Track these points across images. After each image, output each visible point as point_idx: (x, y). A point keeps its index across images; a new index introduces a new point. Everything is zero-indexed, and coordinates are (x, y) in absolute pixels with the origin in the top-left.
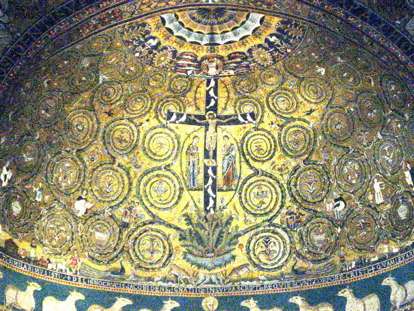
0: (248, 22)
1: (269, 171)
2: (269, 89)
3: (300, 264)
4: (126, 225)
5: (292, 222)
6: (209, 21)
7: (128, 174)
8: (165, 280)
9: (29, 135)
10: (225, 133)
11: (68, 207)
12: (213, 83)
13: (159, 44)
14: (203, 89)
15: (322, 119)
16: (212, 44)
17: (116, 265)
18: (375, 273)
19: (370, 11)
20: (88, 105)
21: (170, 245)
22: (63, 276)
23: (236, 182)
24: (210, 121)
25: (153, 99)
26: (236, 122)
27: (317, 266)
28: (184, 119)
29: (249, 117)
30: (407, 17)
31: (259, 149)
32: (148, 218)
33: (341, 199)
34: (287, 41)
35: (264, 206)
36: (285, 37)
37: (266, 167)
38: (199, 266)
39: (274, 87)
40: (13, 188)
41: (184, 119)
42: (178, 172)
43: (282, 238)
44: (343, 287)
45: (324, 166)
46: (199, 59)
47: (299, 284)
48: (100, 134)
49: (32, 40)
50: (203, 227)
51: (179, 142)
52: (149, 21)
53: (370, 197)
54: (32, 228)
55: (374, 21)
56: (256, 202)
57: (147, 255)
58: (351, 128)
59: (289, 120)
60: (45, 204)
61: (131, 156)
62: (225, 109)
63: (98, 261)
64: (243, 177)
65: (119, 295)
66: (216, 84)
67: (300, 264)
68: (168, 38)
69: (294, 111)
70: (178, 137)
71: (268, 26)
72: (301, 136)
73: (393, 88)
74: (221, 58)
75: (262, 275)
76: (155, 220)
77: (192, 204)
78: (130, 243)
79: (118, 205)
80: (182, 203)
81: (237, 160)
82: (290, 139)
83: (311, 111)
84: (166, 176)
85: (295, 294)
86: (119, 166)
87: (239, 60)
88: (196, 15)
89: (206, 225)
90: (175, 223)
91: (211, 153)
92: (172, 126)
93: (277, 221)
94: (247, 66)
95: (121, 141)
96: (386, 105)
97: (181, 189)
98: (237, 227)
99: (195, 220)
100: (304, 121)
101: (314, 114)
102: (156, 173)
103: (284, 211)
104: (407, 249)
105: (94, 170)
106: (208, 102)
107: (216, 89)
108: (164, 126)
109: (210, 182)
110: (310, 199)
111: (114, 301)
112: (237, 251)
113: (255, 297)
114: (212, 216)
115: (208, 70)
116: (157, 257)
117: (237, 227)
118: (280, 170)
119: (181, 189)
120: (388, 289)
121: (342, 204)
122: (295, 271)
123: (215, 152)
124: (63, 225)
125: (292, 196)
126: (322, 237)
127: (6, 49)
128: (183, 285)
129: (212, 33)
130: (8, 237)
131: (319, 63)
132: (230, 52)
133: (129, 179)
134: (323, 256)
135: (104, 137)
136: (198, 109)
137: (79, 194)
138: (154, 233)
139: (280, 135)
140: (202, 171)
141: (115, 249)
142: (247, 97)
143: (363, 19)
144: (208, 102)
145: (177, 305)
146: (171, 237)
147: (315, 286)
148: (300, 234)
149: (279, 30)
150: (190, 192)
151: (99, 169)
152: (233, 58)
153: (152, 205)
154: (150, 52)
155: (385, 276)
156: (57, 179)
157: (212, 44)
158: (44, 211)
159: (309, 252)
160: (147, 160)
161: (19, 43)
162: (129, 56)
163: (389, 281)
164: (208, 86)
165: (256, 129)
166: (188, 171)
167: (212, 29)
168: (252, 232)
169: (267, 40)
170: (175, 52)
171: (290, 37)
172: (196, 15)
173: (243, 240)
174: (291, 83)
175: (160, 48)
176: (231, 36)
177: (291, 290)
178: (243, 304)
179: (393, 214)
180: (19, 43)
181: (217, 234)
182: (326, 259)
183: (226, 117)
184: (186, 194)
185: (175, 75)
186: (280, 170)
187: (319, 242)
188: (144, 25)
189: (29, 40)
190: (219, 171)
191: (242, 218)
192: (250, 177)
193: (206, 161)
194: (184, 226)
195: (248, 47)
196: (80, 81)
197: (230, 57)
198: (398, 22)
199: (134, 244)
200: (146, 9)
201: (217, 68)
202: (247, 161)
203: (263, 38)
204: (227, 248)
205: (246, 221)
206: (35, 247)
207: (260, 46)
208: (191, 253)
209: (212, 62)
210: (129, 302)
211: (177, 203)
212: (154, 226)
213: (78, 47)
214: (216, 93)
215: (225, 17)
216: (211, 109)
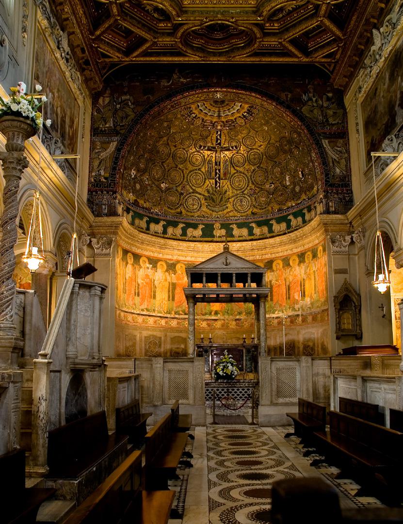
0: (235, 107)
1: (243, 171)
2: (243, 136)
3: (255, 210)
4: (182, 194)
5: (252, 193)
6: (218, 106)
7: (183, 172)
8: (198, 217)
9: (142, 156)
10: (224, 155)
11: (159, 187)
12: (219, 133)
13: (196, 116)
14: (215, 136)
15: (265, 149)
16: (219, 116)
17: (179, 210)
18: (285, 214)
19: (287, 103)
20: (166, 142)
21: (201, 202)
22: (157, 215)
23: (228, 176)
24: (218, 149)
25: (193, 140)
26: (228, 150)
27: (262, 211)
28: (206, 148)
29: (234, 148)
30: (302, 106)
31: (238, 162)
32: (191, 191)
33: (272, 183)
34: (251, 115)
35: (240, 186)
36: (250, 113)
37: (241, 169)
38: (213, 211)
39: (245, 135)
40: (136, 178)
41: (206, 148)
42: (204, 171)
43: (247, 199)
44: (271, 219)
45: (266, 169)
46: (213, 122)
47: (254, 218)
48: (171, 155)
49: (143, 116)
50: (214, 195)
51: (204, 158)
52: (192, 106)
53: (284, 183)
54: (144, 195)
55: (288, 107)
56: (237, 184)
57: (191, 206)
58: (278, 153)
59: (251, 149)
60: (149, 185)
61: (184, 164)
62: (224, 144)
63: (171, 209)
64: (232, 174)
65: (180, 222)
66: (221, 134)
67: (255, 210)
68: (200, 113)
69: (254, 145)
70: (204, 156)
71: (243, 108)
72: (257, 156)
73: (295, 136)
74: (223, 122)
75: (239, 215)
76: (194, 192)
77: (210, 185)
78: (184, 201)
79: (179, 185)
80: (206, 185)
81: (229, 166)
82: (252, 157)
83: (261, 146)
84: (200, 173)
85: (252, 222)
86: (179, 168)
87: (230, 123)
88: (212, 103)
89: (216, 194)
90: (203, 193)
91: (218, 164)
92: (201, 151)
93: (245, 192)
94: (234, 126)
95: (180, 158)
96: (292, 144)
97: (205, 179)
99: (211, 191)
100: (258, 150)
101: (262, 147)
102: (194, 172)
103: (249, 188)
104: (299, 204)
105: (169, 170)
106: (217, 142)
107: (220, 135)
108: (198, 152)
109: (218, 175)
110: (259, 183)
111: (178, 225)
112: (229, 205)
113: (236, 224)
114: (218, 190)
115: (217, 127)
116: (195, 207)
117: (229, 195)
118: (247, 170)
119: (205, 179)
120: (290, 220)
121: (273, 185)
122: (253, 213)
123: (220, 162)
124: (156, 193)
125: (252, 181)
126: (264, 199)
127: (133, 120)
128: (206, 218)
129: (219, 111)
130: (135, 199)
131: (264, 125)
132: (227, 119)
133: (183, 174)
134: (264, 207)
135: (172, 157)
136: (213, 144)
137: (163, 181)
139: (247, 155)
140: (214, 171)
141: (178, 204)
142: (234, 139)
143: (284, 107)
144: (217, 142)
145: (204, 226)
146: (201, 199)
147: (261, 219)
148: (255, 198)
149: (248, 110)
150: (210, 180)
151: (171, 170)
152: (228, 122)
153: (193, 185)
154: (193, 120)
155: (289, 215)
156: (154, 174)
157: (219, 116)
158: (149, 188)
159: (259, 205)
160: (191, 166)
161: (138, 117)
162: (184, 122)
163: (291, 217)
164: (217, 133)
165: (237, 153)
166: (208, 171)
167: (219, 110)
169: (243, 115)
170: (203, 119)
171: (253, 113)
172: (212, 103)
174: (252, 133)
175: (197, 117)
176: (227, 113)
177: (250, 220)
178: (231, 226)
179: (293, 189)
180: (138, 117)
181: (220, 198)
182: (265, 208)
183: (225, 147)
185: (202, 129)
186: (247, 170)
187: (263, 201)
188: (190, 108)
189: (142, 116)
190: (222, 171)
191: (231, 191)
192: (235, 173)
193: (216, 167)
194: (206, 194)
195: (234, 117)
196: (163, 132)
197: (227, 122)
198: (298, 108)
199: (186, 202)
200: (191, 101)
201: (221, 126)
202: (233, 167)
203: (241, 113)
204: (225, 203)
205: (232, 192)
206: (146, 203)
207: (240, 117)
208: (209, 205)
209: (219, 123)
210: (184, 225)
211: (203, 185)
212: (194, 194)
213: (162, 118)
214: (220, 137)
215: (225, 104)
216: (218, 144)
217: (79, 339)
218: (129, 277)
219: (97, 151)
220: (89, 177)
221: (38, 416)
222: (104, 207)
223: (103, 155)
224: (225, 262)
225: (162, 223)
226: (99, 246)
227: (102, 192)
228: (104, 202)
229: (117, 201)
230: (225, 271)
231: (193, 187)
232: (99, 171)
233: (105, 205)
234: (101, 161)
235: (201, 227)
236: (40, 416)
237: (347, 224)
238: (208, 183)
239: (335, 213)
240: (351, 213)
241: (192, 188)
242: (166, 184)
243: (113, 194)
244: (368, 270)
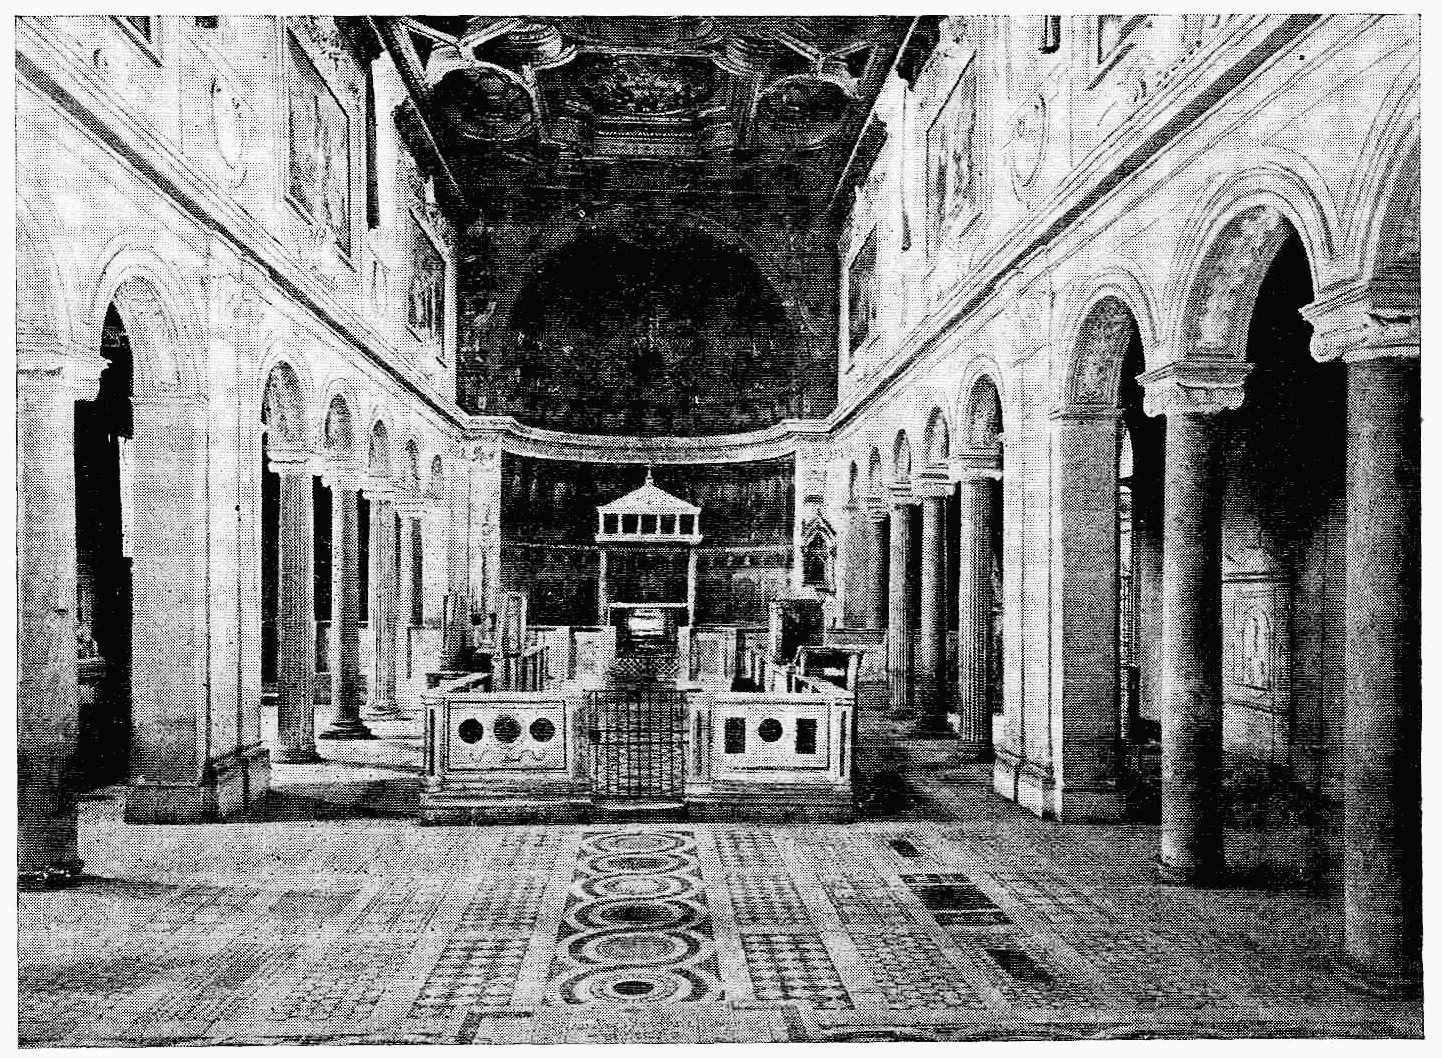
223: (481, 320)
239: (812, 415)
240: (839, 413)
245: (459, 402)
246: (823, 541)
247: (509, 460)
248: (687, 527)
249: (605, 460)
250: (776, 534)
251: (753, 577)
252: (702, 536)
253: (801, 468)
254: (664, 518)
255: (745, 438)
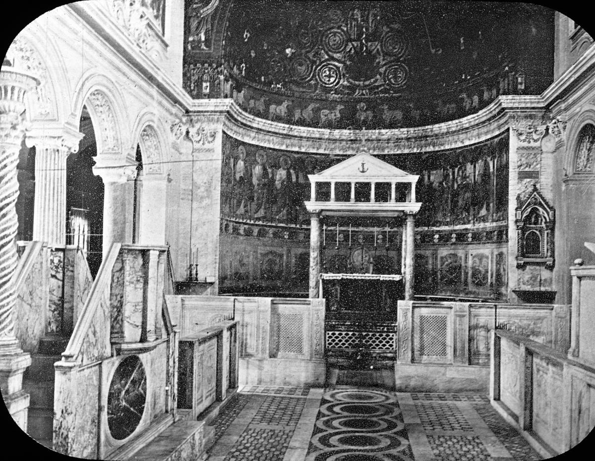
4: (314, 62)
32: (327, 57)
42: (345, 29)
98: (379, 62)
117: (379, 62)
138: (331, 66)
145: (343, 107)
146: (341, 69)
168: (387, 66)
173: (382, 70)
184: (350, 44)
191: (382, 58)
217: (127, 318)
218: (241, 177)
219: (195, 6)
220: (185, 43)
221: (61, 433)
222: (204, 85)
224: (361, 170)
225: (285, 104)
226: (199, 137)
227: (203, 65)
228: (205, 77)
229: (222, 77)
230: (362, 180)
231: (330, 53)
232: (197, 35)
233: (206, 81)
234: (201, 21)
235: (340, 107)
236: (62, 434)
237: (541, 108)
238: (351, 46)
239: (525, 92)
240: (551, 92)
241: (328, 55)
242: (292, 49)
243: (217, 68)
244: (566, 175)
245: (186, 86)
246: (538, 216)
247: (231, 144)
248: (401, 198)
249: (321, 151)
250: (483, 212)
251: (461, 253)
252: (420, 204)
253: (514, 143)
254: (378, 185)
255: (453, 124)
